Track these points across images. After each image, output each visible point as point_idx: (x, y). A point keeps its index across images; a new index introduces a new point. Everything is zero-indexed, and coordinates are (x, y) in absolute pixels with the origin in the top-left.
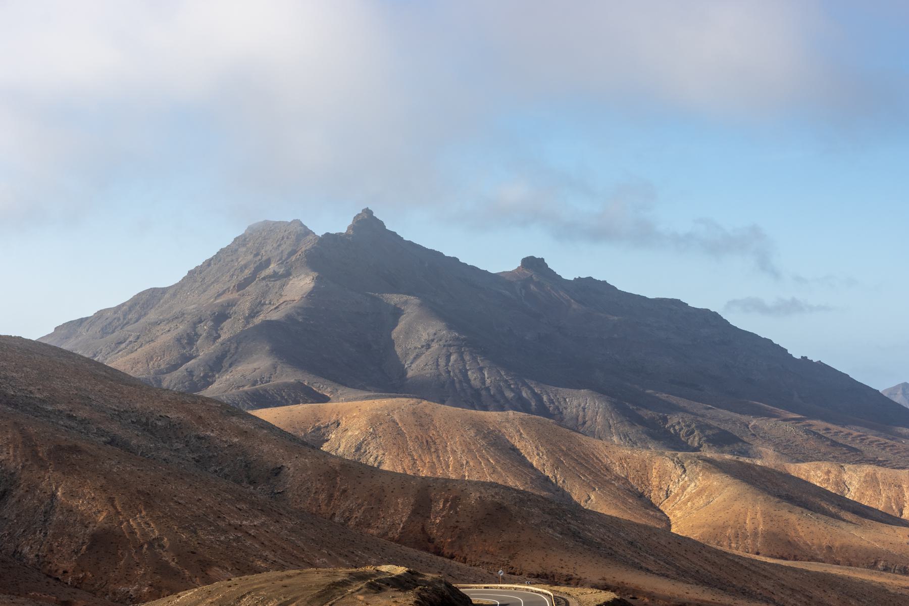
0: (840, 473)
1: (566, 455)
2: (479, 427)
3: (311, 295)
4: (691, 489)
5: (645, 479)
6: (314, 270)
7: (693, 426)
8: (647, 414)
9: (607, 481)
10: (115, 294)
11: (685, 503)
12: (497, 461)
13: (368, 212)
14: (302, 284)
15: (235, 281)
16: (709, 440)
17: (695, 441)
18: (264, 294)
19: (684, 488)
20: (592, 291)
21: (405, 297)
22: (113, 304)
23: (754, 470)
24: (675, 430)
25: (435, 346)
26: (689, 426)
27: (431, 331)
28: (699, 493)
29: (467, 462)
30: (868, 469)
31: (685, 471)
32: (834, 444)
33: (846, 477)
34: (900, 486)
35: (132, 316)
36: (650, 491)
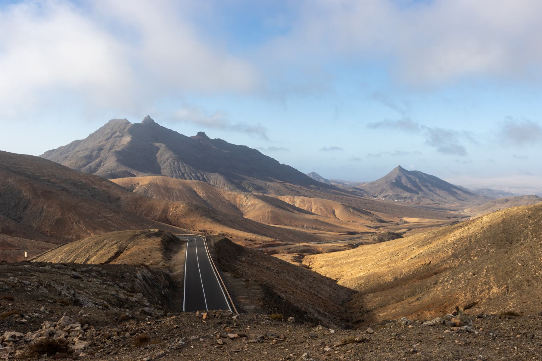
1: (211, 193)
3: (130, 142)
6: (131, 135)
8: (236, 181)
10: (64, 141)
13: (149, 117)
14: (127, 139)
15: (105, 138)
16: (255, 189)
18: (115, 142)
20: (219, 142)
21: (160, 144)
22: (64, 145)
25: (170, 159)
27: (169, 154)
30: (302, 198)
32: (292, 190)
33: (295, 200)
35: (71, 149)
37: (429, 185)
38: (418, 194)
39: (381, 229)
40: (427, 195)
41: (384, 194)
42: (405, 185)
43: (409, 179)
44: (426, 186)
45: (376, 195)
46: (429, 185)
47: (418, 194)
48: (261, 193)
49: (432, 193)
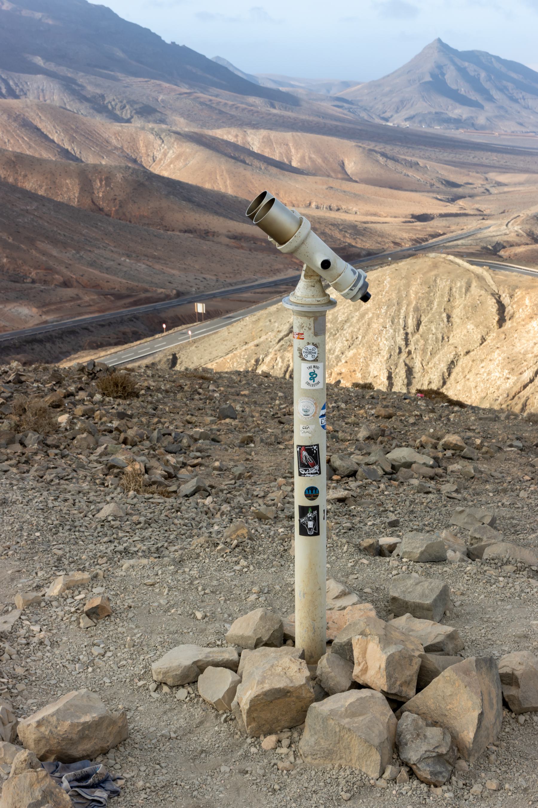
0: (245, 136)
1: (76, 132)
2: (8, 112)
4: (171, 154)
5: (136, 149)
7: (125, 102)
9: (109, 151)
11: (169, 165)
12: (30, 139)
16: (137, 113)
17: (126, 114)
19: (165, 154)
23: (206, 138)
24: (111, 105)
26: (121, 102)
28: (178, 157)
29: (9, 141)
30: (263, 133)
31: (163, 142)
32: (221, 112)
33: (249, 139)
34: (287, 145)
36: (141, 157)
37: (510, 85)
38: (481, 107)
39: (461, 202)
40: (506, 111)
41: (405, 113)
42: (454, 87)
43: (462, 71)
44: (502, 90)
45: (388, 115)
46: (510, 85)
47: (481, 107)
48: (155, 122)
49: (516, 106)
